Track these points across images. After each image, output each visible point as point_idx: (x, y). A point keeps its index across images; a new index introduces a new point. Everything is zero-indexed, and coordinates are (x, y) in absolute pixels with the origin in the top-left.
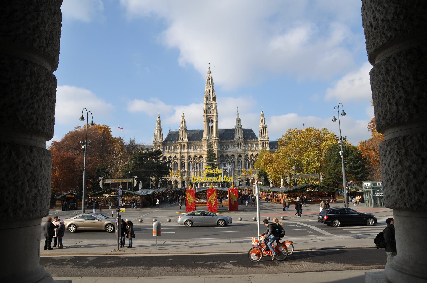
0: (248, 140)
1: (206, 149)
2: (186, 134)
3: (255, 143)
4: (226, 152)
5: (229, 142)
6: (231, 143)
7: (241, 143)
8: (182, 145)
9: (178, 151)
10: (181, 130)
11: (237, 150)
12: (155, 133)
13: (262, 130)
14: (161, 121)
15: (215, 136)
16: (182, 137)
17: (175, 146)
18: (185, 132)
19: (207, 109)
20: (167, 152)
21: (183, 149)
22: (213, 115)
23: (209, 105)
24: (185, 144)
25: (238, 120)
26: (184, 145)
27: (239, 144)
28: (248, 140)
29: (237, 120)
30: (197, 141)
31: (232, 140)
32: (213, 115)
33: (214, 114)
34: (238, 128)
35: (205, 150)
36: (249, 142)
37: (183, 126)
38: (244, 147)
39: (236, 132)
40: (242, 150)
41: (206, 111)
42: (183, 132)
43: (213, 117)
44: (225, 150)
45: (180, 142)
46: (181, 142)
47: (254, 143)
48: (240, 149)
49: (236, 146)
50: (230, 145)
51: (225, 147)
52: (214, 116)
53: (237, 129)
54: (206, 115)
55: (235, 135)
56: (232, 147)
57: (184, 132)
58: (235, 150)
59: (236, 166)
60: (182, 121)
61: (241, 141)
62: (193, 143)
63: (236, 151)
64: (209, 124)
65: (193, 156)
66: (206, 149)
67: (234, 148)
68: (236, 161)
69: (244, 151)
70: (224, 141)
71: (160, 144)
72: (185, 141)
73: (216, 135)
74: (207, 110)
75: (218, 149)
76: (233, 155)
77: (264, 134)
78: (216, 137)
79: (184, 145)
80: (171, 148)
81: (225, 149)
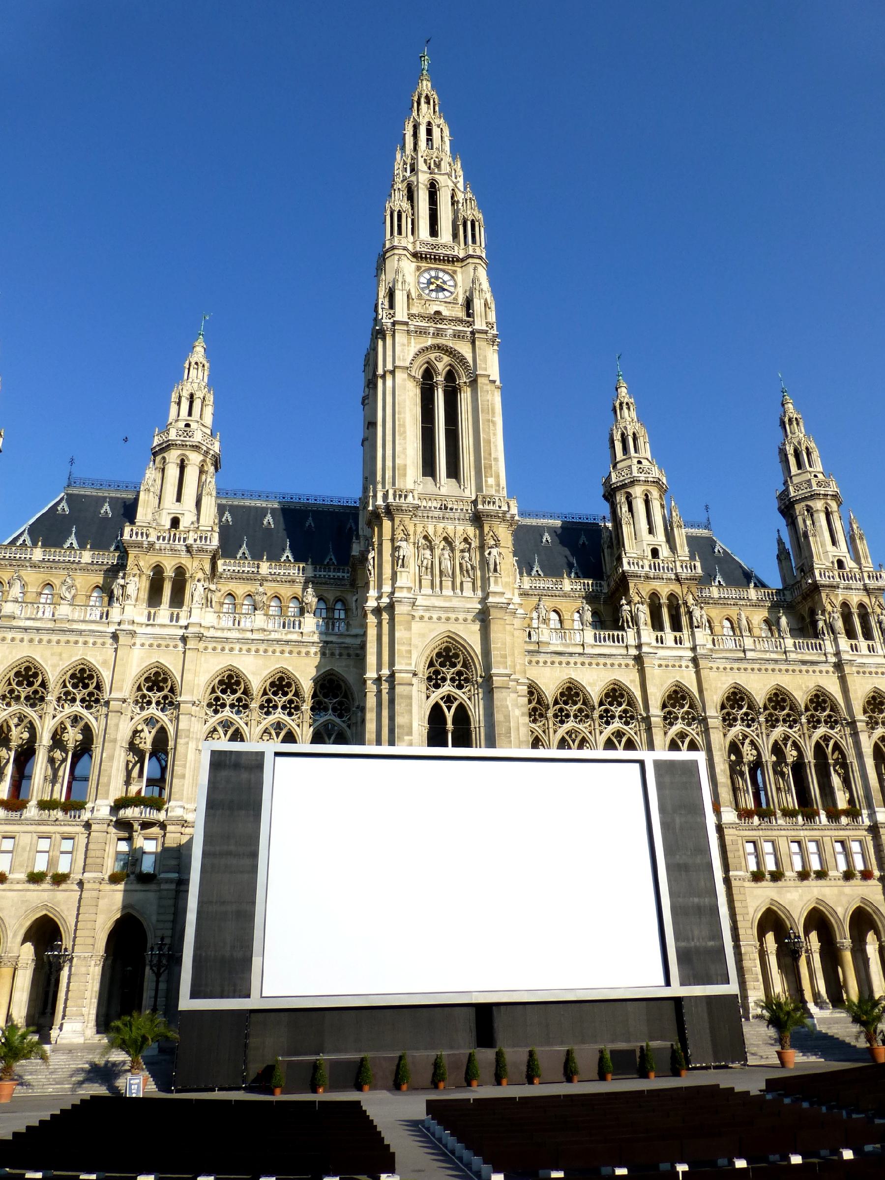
4: (557, 659)
7: (672, 597)
8: (158, 570)
19: (414, 295)
21: (164, 612)
23: (424, 265)
24: (192, 566)
26: (180, 571)
27: (664, 601)
32: (457, 336)
37: (187, 425)
42: (182, 467)
45: (139, 545)
46: (151, 545)
54: (406, 324)
79: (180, 571)
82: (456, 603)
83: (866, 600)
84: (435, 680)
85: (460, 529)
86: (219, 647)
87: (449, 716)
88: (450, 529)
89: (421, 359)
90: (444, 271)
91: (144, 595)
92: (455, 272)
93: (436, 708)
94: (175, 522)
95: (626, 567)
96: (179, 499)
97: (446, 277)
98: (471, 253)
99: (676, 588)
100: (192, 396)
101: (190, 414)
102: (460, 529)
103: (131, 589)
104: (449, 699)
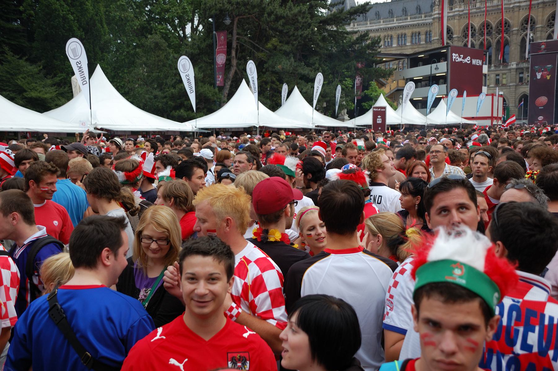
9: (510, 4)
86: (551, 4)
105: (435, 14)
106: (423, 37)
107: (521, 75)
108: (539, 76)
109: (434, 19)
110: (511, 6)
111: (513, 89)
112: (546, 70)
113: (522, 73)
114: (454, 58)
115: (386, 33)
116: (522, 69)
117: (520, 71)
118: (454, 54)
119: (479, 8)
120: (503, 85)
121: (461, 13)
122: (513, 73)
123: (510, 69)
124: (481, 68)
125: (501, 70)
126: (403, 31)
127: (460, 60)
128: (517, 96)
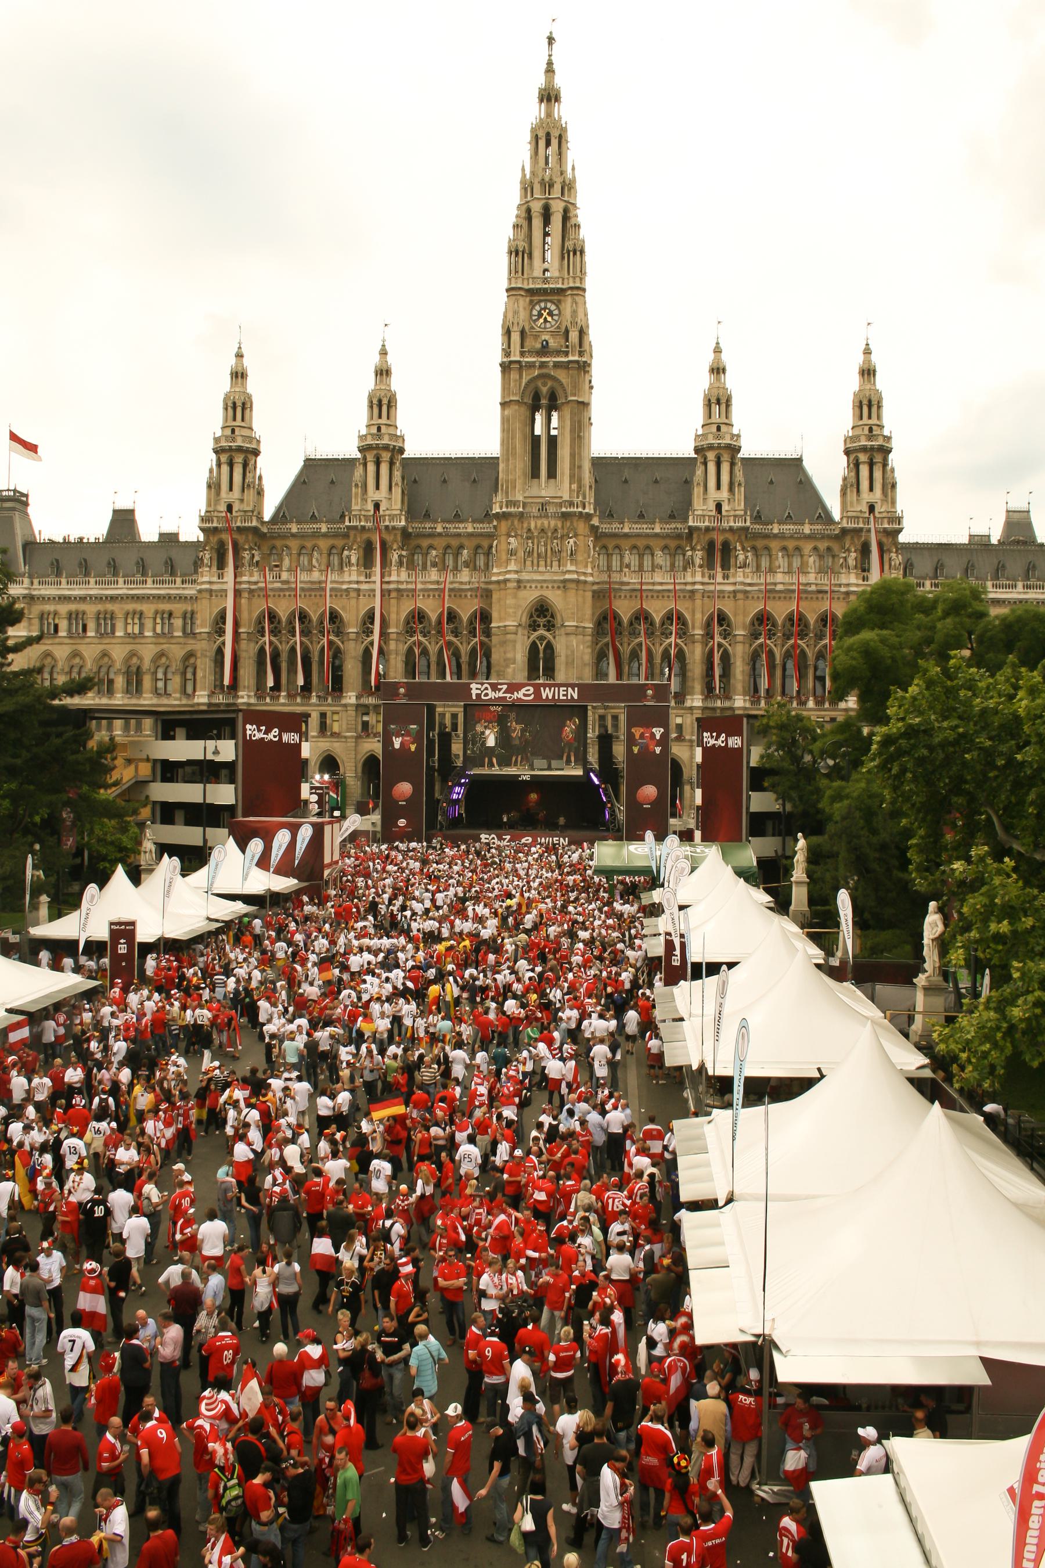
0: (776, 526)
1: (509, 572)
2: (397, 474)
3: (815, 549)
5: (657, 535)
6: (668, 542)
9: (343, 583)
10: (370, 457)
11: (703, 584)
12: (211, 471)
13: (864, 470)
14: (250, 397)
15: (566, 497)
16: (373, 495)
17: (334, 551)
18: (392, 464)
19: (527, 329)
20: (279, 585)
22: (557, 365)
23: (535, 298)
24: (389, 538)
25: (718, 402)
27: (718, 546)
28: (776, 526)
29: (713, 400)
30: (461, 526)
31: (673, 526)
33: (571, 358)
34: (711, 447)
35: (498, 582)
36: (775, 536)
37: (379, 429)
38: (747, 570)
39: (699, 472)
40: (731, 588)
41: (516, 337)
42: (378, 464)
43: (561, 375)
44: (628, 583)
45: (355, 528)
46: (363, 527)
47: (807, 547)
48: (719, 579)
49: (698, 561)
50: (659, 553)
51: (628, 566)
52: (567, 368)
53: (711, 456)
54: (519, 362)
55: (698, 491)
56: (673, 565)
57: (384, 468)
58: (689, 588)
59: (689, 684)
60: (375, 401)
61: (731, 529)
62: (440, 535)
63: (693, 592)
64: (539, 418)
65: (432, 610)
66: (509, 572)
67: (685, 569)
68: (696, 655)
69: (746, 592)
70: (626, 530)
71: (241, 539)
72: (387, 523)
73: (574, 486)
74: (523, 333)
75: (585, 574)
76: (672, 617)
77: (871, 489)
78: (571, 504)
80: (310, 561)
81: (625, 579)
82: (547, 577)
83: (884, 540)
84: (533, 626)
85: (553, 523)
87: (541, 648)
88: (546, 523)
89: (532, 386)
90: (551, 301)
91: (361, 562)
92: (559, 301)
93: (534, 644)
94: (377, 506)
95: (691, 523)
96: (378, 488)
97: (553, 307)
98: (571, 285)
99: (729, 536)
100: (380, 401)
101: (380, 417)
102: (553, 523)
103: (354, 560)
104: (542, 638)
105: (203, 583)
106: (178, 623)
107: (365, 718)
108: (397, 743)
109: (200, 591)
110: (345, 587)
111: (351, 744)
112: (408, 734)
113: (367, 714)
114: (248, 732)
115: (100, 607)
116: (366, 706)
117: (363, 709)
118: (248, 727)
119: (287, 582)
120: (334, 735)
121: (253, 587)
122: (352, 713)
123: (345, 706)
124: (297, 747)
125: (329, 705)
126: (138, 607)
127: (259, 736)
128: (359, 757)
